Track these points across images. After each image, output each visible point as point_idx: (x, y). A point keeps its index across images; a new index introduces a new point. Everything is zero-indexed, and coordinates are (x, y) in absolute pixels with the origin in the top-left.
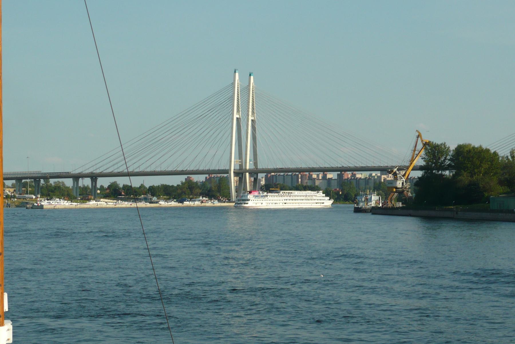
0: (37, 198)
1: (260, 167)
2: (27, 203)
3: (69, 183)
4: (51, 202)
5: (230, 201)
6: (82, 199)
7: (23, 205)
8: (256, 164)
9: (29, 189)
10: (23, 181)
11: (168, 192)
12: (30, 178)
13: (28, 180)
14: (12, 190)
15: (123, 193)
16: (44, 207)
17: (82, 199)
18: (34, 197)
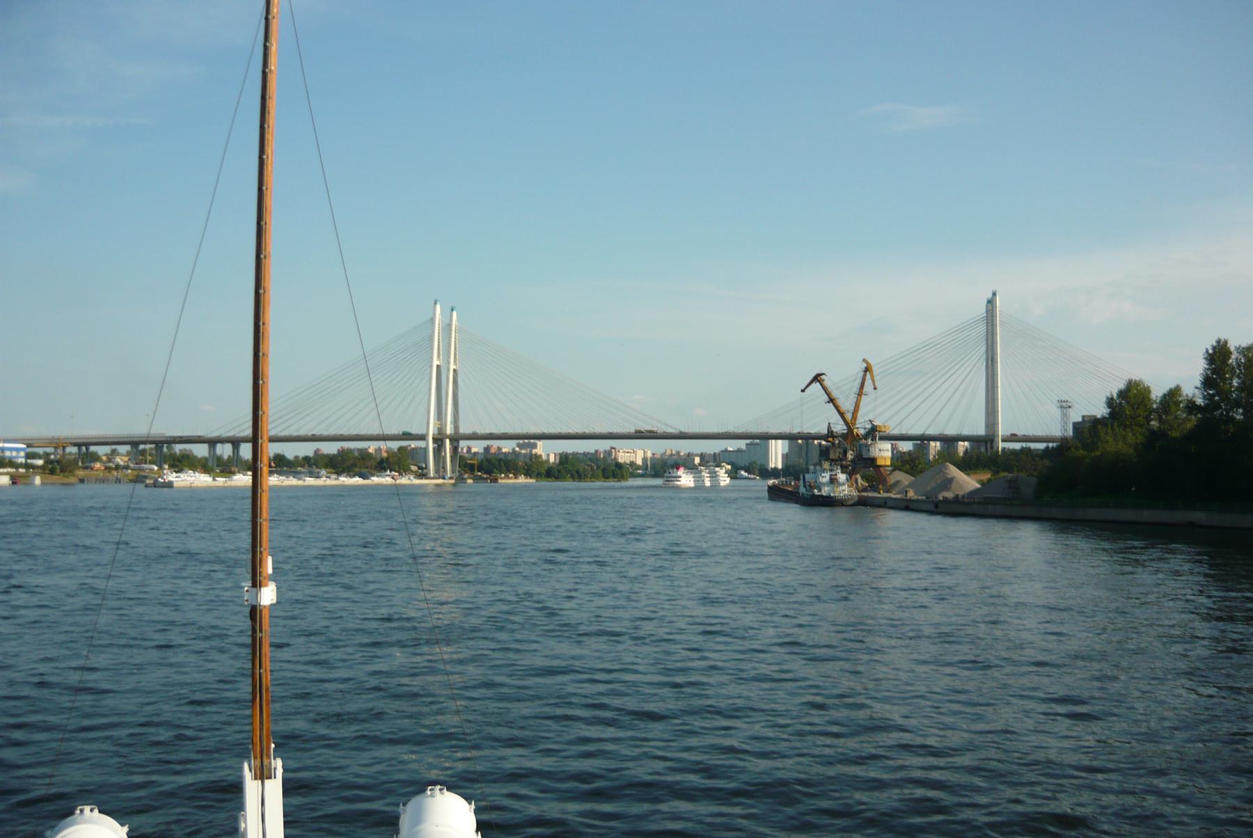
0: (161, 468)
1: (464, 429)
2: (146, 477)
3: (201, 451)
4: (181, 475)
5: (422, 475)
6: (222, 472)
7: (139, 479)
8: (456, 427)
9: (149, 458)
10: (141, 447)
11: (338, 464)
12: (151, 443)
13: (148, 446)
14: (126, 459)
16: (175, 484)
17: (222, 472)
18: (156, 468)
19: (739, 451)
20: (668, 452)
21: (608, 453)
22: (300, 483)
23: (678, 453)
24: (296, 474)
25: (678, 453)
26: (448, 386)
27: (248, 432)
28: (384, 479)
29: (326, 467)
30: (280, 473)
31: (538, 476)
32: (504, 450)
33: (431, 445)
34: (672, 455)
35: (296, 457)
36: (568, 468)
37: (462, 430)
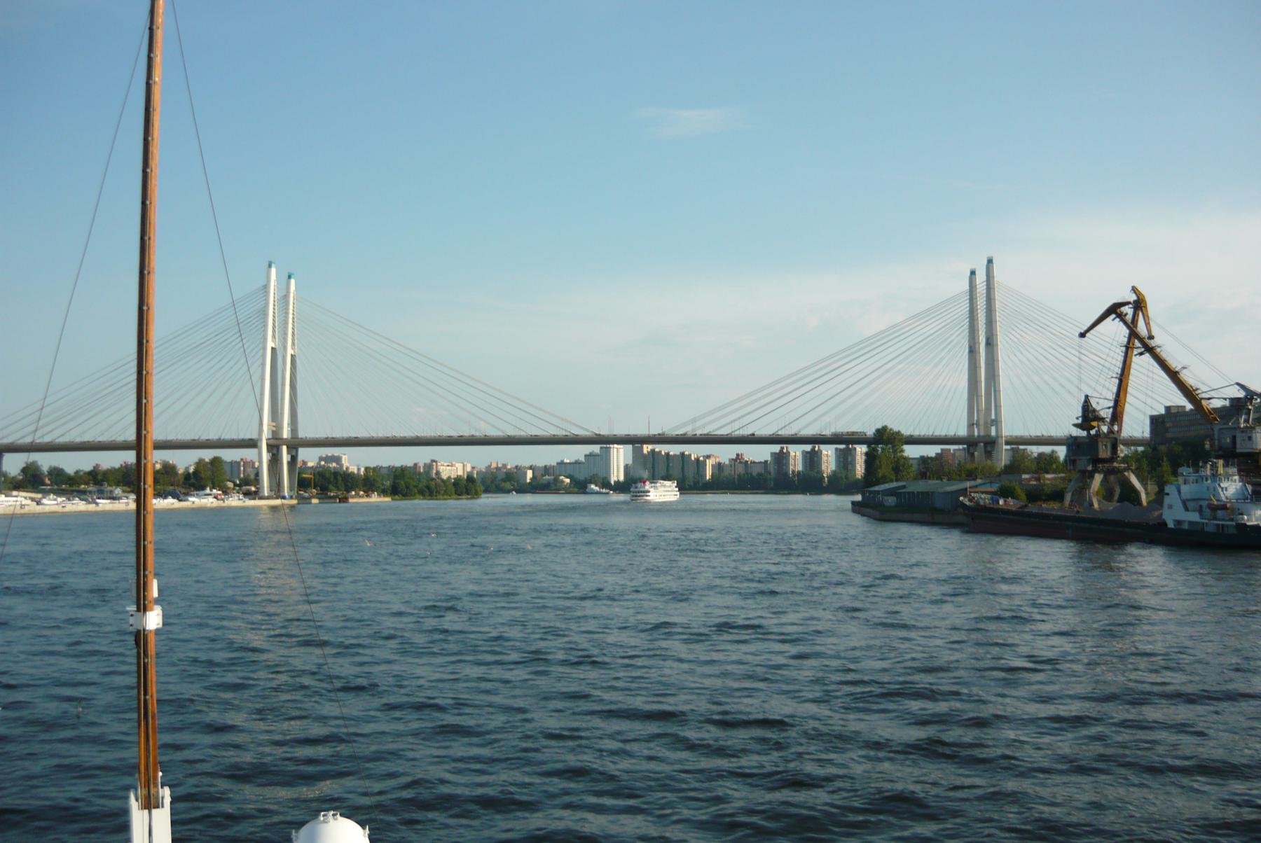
15: (47, 481)
19: (577, 463)
20: (494, 465)
21: (429, 467)
22: (92, 507)
23: (505, 466)
24: (82, 494)
25: (505, 466)
26: (284, 380)
27: (131, 435)
28: (205, 500)
29: (117, 485)
30: (59, 493)
31: (384, 492)
32: (310, 464)
33: (265, 456)
34: (497, 468)
35: (77, 472)
36: (401, 484)
37: (302, 434)
